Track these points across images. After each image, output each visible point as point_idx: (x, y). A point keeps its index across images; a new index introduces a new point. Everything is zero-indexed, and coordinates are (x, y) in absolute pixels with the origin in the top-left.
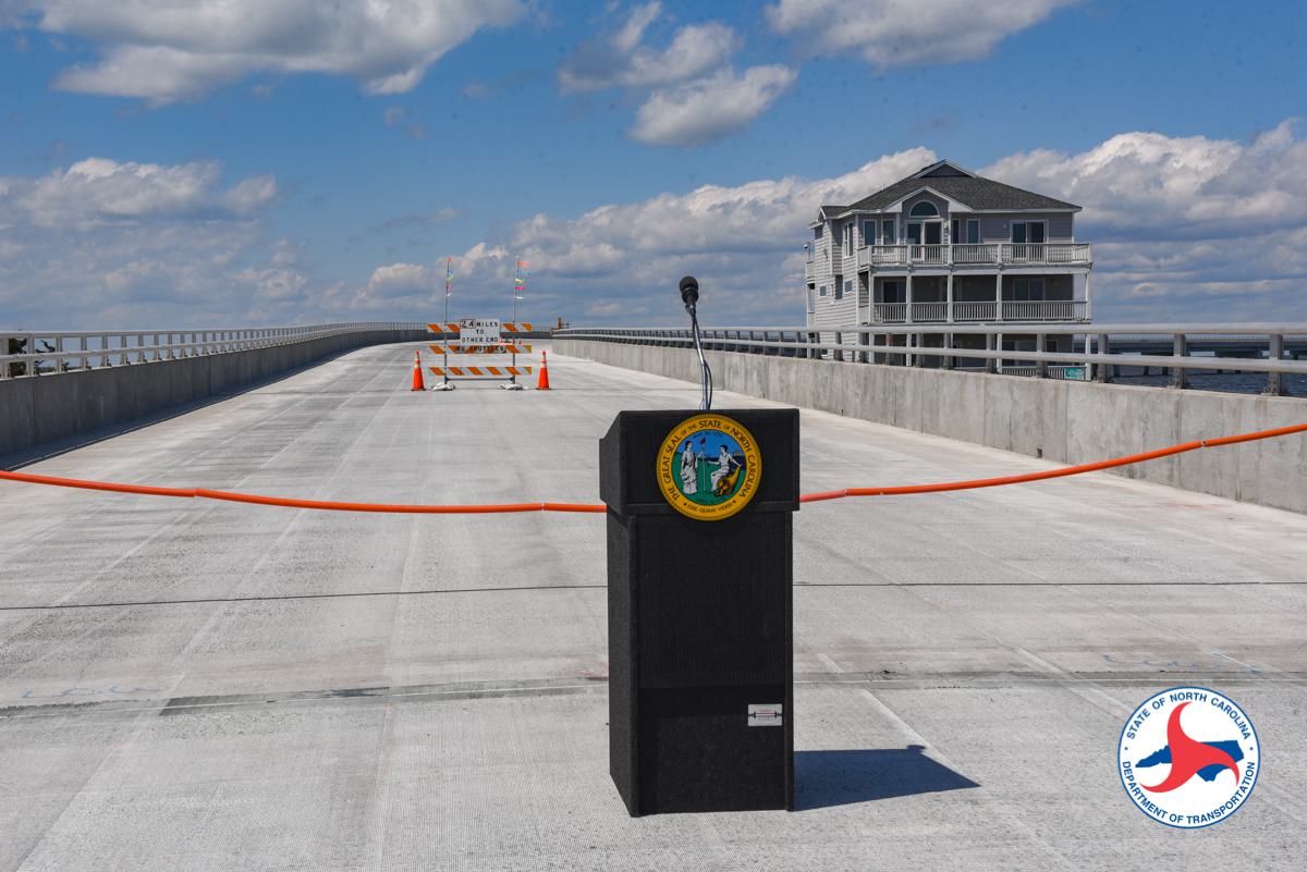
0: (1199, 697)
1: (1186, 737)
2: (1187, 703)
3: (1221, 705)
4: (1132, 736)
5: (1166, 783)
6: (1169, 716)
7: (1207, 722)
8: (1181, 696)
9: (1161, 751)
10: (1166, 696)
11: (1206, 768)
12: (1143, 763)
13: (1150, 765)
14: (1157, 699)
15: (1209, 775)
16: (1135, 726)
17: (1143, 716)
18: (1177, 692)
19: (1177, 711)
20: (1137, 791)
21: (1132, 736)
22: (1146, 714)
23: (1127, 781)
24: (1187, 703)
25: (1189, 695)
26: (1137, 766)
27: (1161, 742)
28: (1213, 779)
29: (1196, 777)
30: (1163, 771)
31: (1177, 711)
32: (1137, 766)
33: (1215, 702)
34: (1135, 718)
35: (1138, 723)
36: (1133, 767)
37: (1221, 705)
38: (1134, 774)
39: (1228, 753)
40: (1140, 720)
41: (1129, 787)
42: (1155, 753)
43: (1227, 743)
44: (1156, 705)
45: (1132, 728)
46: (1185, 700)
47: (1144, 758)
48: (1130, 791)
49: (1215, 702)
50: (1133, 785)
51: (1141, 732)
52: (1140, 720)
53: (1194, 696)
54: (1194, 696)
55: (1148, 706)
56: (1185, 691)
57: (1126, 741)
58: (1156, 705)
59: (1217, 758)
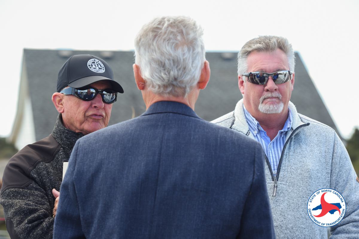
0: (329, 191)
1: (326, 202)
2: (326, 193)
4: (311, 202)
5: (320, 215)
6: (321, 196)
8: (324, 191)
9: (319, 206)
10: (320, 191)
11: (331, 210)
12: (314, 209)
13: (316, 210)
14: (318, 192)
15: (332, 212)
16: (312, 199)
17: (314, 196)
18: (323, 190)
19: (323, 195)
20: (312, 217)
21: (311, 202)
22: (315, 196)
23: (309, 214)
24: (326, 193)
25: (327, 191)
26: (312, 210)
27: (319, 203)
28: (333, 214)
29: (329, 213)
30: (319, 211)
31: (323, 195)
32: (312, 210)
33: (334, 192)
34: (312, 197)
35: (312, 198)
36: (311, 210)
37: (335, 193)
38: (311, 212)
39: (337, 206)
40: (313, 197)
41: (310, 216)
42: (317, 206)
43: (337, 204)
44: (318, 193)
45: (311, 199)
46: (326, 192)
47: (314, 208)
48: (310, 217)
49: (334, 192)
50: (311, 215)
51: (313, 201)
52: (313, 197)
53: (328, 191)
54: (328, 191)
55: (315, 194)
56: (325, 189)
57: (309, 203)
58: (318, 193)
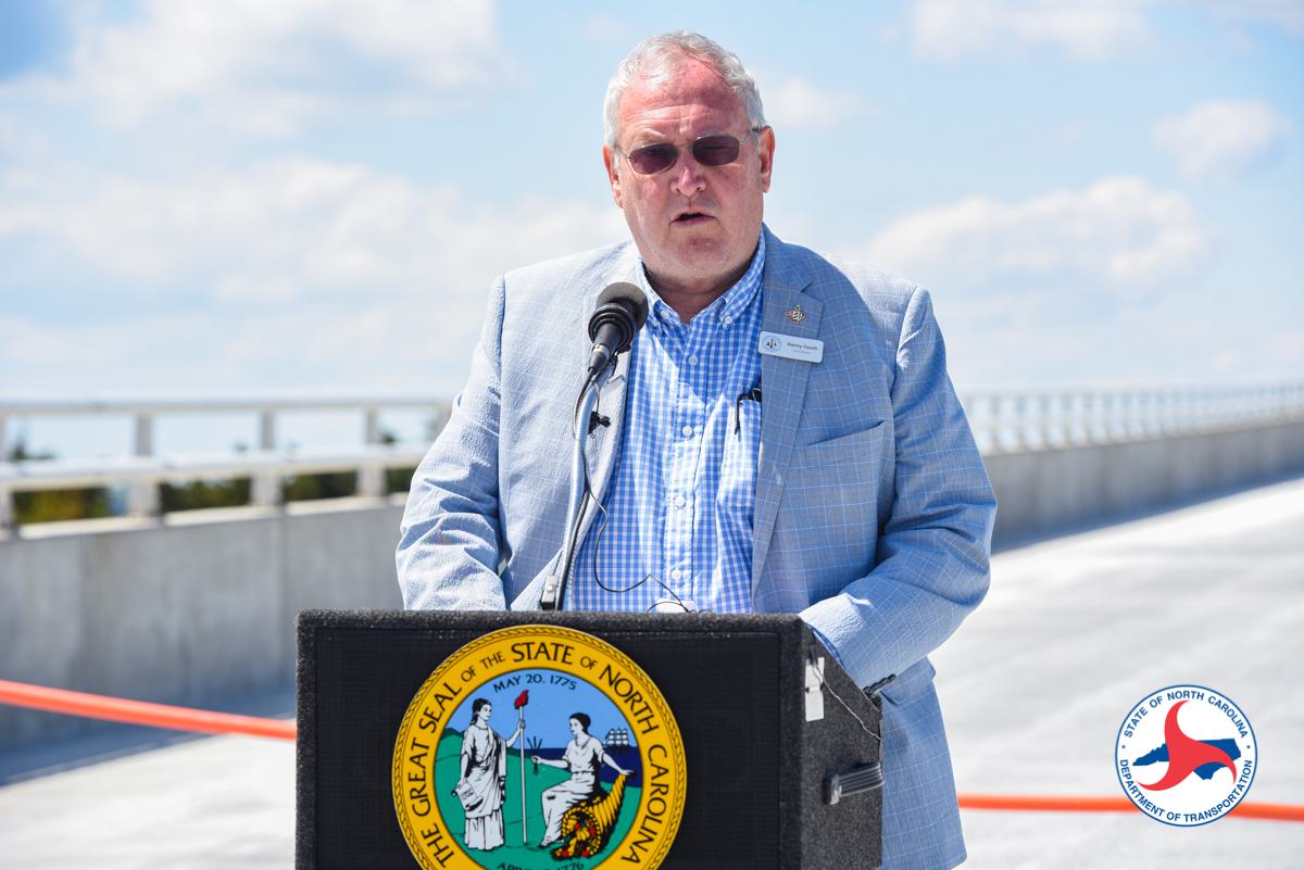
0: (1196, 695)
1: (1184, 736)
2: (1184, 702)
3: (1219, 703)
4: (1129, 734)
5: (1163, 781)
6: (1166, 714)
7: (1202, 723)
8: (1179, 695)
9: (1158, 749)
10: (1164, 695)
11: (1203, 766)
12: (1141, 762)
13: (1147, 764)
14: (1155, 697)
15: (1206, 773)
16: (1132, 725)
17: (1140, 714)
18: (1174, 690)
19: (1175, 710)
20: (1135, 789)
21: (1129, 734)
22: (1143, 712)
23: (1124, 780)
24: (1184, 702)
25: (1186, 694)
26: (1135, 764)
27: (1158, 740)
28: (1210, 777)
29: (1193, 775)
30: (1160, 769)
31: (1175, 710)
32: (1135, 764)
33: (1212, 700)
34: (1132, 716)
35: (1135, 722)
36: (1130, 765)
37: (1219, 703)
38: (1131, 772)
39: (1225, 752)
40: (1137, 718)
41: (1126, 785)
42: (1153, 752)
43: (1224, 741)
44: (1154, 703)
45: (1129, 726)
46: (1183, 699)
47: (1141, 756)
48: (1128, 789)
49: (1212, 700)
50: (1130, 783)
51: (1138, 730)
52: (1137, 718)
53: (1191, 695)
54: (1191, 695)
55: (1146, 705)
56: (1182, 690)
58: (1154, 703)
59: (1215, 756)
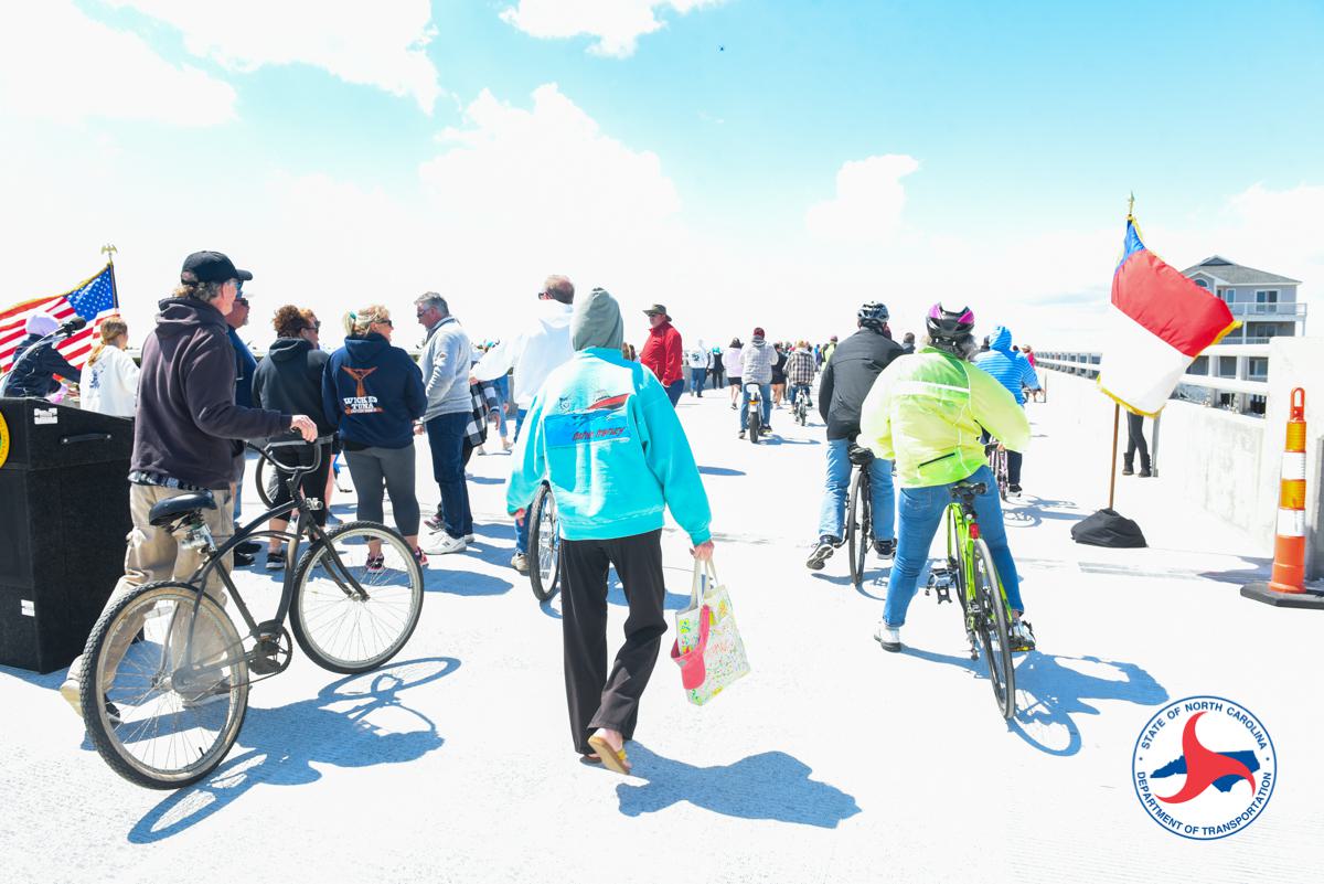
0: (1214, 706)
1: (1202, 748)
2: (1202, 713)
3: (1237, 715)
4: (1146, 746)
5: (1181, 793)
6: (1184, 726)
8: (1197, 706)
9: (1176, 761)
11: (1221, 779)
12: (1158, 774)
13: (1165, 776)
15: (1225, 785)
16: (1149, 736)
17: (1158, 726)
19: (1193, 721)
20: (1152, 802)
21: (1146, 746)
22: (1161, 724)
23: (1142, 792)
24: (1202, 713)
26: (1152, 776)
27: (1176, 752)
28: (1229, 790)
29: (1212, 788)
30: (1178, 782)
31: (1193, 721)
32: (1152, 776)
33: (1231, 711)
35: (1152, 733)
36: (1147, 777)
37: (1237, 715)
38: (1149, 785)
40: (1154, 730)
41: (1143, 798)
42: (1170, 764)
43: (1242, 753)
44: (1171, 715)
46: (1201, 710)
47: (1159, 768)
48: (1145, 802)
49: (1231, 711)
50: (1148, 796)
52: (1154, 730)
53: (1209, 706)
54: (1209, 706)
58: (1171, 715)
